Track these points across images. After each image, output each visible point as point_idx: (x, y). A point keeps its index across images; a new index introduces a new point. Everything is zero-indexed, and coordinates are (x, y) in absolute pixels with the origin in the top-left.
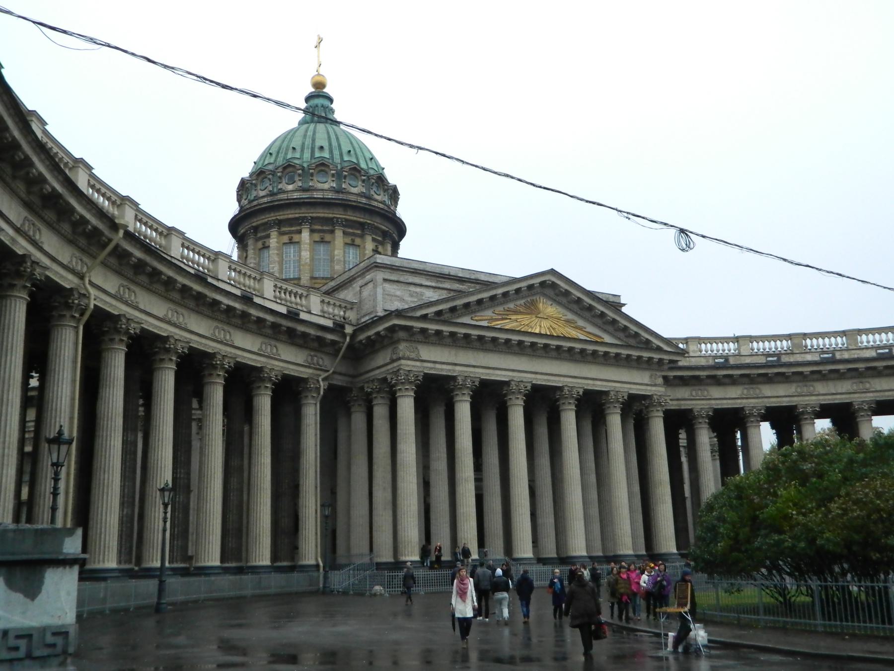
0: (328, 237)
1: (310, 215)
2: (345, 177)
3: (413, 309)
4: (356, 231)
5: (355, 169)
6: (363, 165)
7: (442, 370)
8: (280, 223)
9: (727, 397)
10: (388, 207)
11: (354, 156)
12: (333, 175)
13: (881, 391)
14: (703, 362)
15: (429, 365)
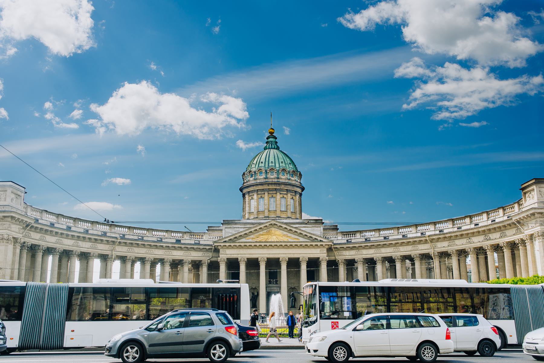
0: (263, 195)
1: (256, 189)
2: (268, 173)
3: (220, 240)
4: (274, 192)
5: (272, 169)
6: (277, 165)
7: (234, 256)
8: (249, 192)
9: (369, 253)
10: (289, 179)
11: (274, 163)
12: (264, 173)
13: (421, 250)
14: (361, 240)
15: (229, 255)
